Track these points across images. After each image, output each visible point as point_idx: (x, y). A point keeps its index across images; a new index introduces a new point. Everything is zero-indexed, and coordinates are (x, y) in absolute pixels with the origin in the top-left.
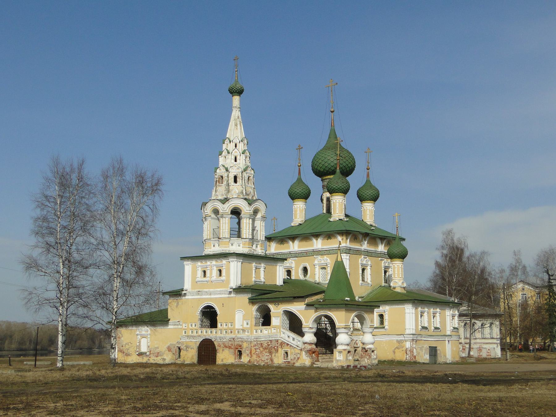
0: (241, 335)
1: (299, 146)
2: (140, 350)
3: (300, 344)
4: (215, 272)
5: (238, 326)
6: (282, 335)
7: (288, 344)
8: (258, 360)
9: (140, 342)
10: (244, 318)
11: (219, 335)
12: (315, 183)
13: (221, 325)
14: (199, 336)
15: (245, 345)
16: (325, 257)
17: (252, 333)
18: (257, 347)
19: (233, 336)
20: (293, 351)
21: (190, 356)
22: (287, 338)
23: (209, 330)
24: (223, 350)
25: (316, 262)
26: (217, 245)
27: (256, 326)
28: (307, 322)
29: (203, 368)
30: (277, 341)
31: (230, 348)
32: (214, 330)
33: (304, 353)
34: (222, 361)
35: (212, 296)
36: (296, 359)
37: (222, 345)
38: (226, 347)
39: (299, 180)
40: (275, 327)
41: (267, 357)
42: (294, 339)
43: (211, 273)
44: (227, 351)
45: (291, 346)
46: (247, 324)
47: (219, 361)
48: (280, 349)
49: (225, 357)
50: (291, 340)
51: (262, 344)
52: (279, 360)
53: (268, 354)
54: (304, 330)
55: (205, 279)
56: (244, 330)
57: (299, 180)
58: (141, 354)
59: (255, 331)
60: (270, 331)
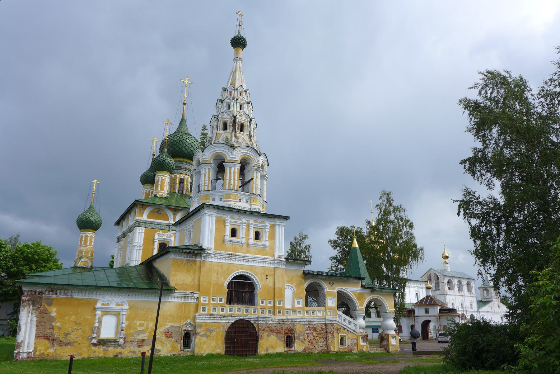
0: (292, 316)
2: (99, 336)
5: (288, 304)
6: (338, 319)
7: (344, 329)
8: (311, 347)
9: (100, 322)
10: (295, 295)
13: (262, 302)
15: (298, 329)
18: (309, 332)
19: (279, 317)
20: (350, 335)
21: (210, 344)
22: (343, 323)
23: (243, 307)
24: (268, 336)
28: (362, 305)
29: (234, 361)
30: (333, 324)
31: (278, 332)
32: (251, 308)
34: (267, 350)
35: (250, 264)
36: (353, 345)
38: (272, 331)
40: (330, 308)
41: (321, 344)
42: (349, 323)
44: (273, 338)
45: (348, 330)
46: (298, 303)
47: (262, 351)
48: (336, 334)
49: (271, 344)
51: (315, 328)
52: (335, 347)
53: (323, 340)
56: (294, 311)
58: (103, 342)
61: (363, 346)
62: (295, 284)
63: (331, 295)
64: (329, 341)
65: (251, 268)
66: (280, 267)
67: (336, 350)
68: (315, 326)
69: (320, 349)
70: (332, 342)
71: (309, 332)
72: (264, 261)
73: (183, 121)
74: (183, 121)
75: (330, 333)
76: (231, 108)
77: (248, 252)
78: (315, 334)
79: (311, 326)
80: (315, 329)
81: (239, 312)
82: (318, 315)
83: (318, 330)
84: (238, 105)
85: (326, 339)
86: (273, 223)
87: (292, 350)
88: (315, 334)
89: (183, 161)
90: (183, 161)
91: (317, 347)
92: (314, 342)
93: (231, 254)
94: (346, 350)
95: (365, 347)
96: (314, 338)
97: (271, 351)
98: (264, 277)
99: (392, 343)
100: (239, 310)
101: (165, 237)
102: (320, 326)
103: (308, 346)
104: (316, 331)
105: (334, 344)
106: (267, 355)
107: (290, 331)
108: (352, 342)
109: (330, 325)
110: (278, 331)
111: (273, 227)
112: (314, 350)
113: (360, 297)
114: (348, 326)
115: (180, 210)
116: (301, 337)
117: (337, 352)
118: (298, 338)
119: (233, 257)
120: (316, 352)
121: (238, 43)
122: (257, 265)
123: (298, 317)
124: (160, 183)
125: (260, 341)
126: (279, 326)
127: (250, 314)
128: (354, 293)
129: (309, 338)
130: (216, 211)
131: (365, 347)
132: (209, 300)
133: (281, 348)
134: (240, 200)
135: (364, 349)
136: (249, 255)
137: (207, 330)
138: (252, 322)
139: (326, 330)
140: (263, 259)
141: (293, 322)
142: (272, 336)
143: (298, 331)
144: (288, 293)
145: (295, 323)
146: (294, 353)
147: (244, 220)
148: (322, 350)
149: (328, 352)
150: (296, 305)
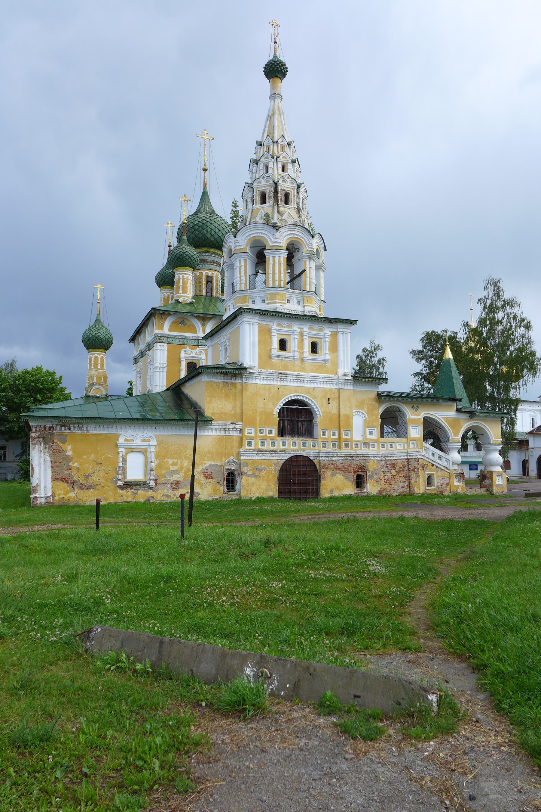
0: (363, 451)
2: (125, 477)
5: (357, 436)
6: (424, 453)
7: (433, 465)
8: (388, 488)
9: (124, 461)
10: (367, 424)
13: (324, 434)
14: (284, 451)
15: (371, 466)
18: (386, 469)
19: (346, 451)
20: (440, 473)
21: (260, 485)
22: (432, 458)
23: (299, 441)
24: (333, 475)
26: (294, 301)
28: (456, 434)
29: (291, 505)
30: (417, 460)
31: (345, 470)
32: (310, 442)
34: (332, 492)
35: (306, 385)
37: (331, 466)
38: (338, 469)
40: (414, 439)
41: (402, 484)
42: (440, 457)
44: (339, 478)
45: (437, 467)
46: (371, 433)
47: (325, 493)
48: (421, 472)
49: (335, 485)
51: (393, 464)
52: (420, 487)
53: (404, 480)
56: (366, 444)
58: (130, 485)
61: (458, 487)
62: (366, 410)
63: (415, 422)
64: (413, 481)
65: (308, 390)
66: (346, 388)
67: (422, 491)
68: (394, 462)
69: (401, 490)
70: (416, 482)
71: (386, 469)
72: (324, 380)
73: (205, 195)
74: (205, 195)
75: (414, 470)
76: (270, 171)
77: (303, 370)
78: (394, 472)
79: (388, 463)
80: (393, 466)
81: (294, 446)
82: (397, 448)
83: (398, 467)
84: (280, 166)
85: (409, 479)
86: (335, 330)
87: (364, 492)
88: (394, 472)
89: (209, 252)
90: (209, 252)
91: (396, 487)
92: (393, 482)
93: (281, 373)
94: (435, 492)
95: (460, 488)
96: (393, 477)
97: (336, 494)
98: (325, 401)
99: (497, 483)
100: (294, 444)
101: (193, 355)
102: (400, 462)
103: (384, 487)
104: (395, 468)
105: (419, 484)
106: (333, 499)
107: (361, 468)
108: (442, 482)
109: (413, 461)
110: (345, 469)
111: (335, 335)
112: (392, 492)
113: (454, 423)
114: (438, 461)
115: (210, 319)
116: (375, 476)
117: (423, 494)
118: (372, 477)
119: (283, 377)
120: (396, 494)
122: (315, 386)
123: (370, 451)
124: (181, 284)
125: (323, 482)
126: (347, 463)
127: (310, 448)
128: (447, 420)
129: (386, 478)
130: (257, 317)
131: (460, 488)
132: (256, 432)
133: (350, 490)
134: (289, 302)
135: (459, 490)
137: (256, 469)
138: (312, 458)
139: (408, 467)
140: (324, 378)
141: (365, 458)
142: (337, 475)
143: (371, 469)
144: (358, 421)
145: (367, 458)
146: (367, 496)
147: (296, 327)
148: (403, 492)
149: (411, 494)
150: (369, 437)
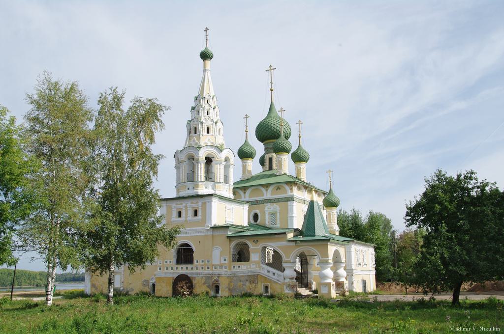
1: (246, 115)
3: (281, 279)
4: (191, 213)
5: (216, 261)
10: (222, 254)
11: (195, 271)
12: (259, 148)
13: (197, 262)
16: (275, 204)
17: (230, 269)
19: (210, 271)
22: (268, 274)
25: (266, 209)
27: (233, 262)
32: (189, 266)
33: (285, 287)
39: (246, 143)
40: (255, 262)
43: (187, 214)
46: (225, 260)
50: (271, 275)
54: (284, 265)
55: (180, 219)
57: (246, 143)
59: (232, 267)
60: (249, 267)
81: (183, 269)
121: (205, 56)
122: (193, 235)
123: (223, 271)
127: (179, 270)
134: (188, 189)
136: (189, 229)
150: (223, 262)
